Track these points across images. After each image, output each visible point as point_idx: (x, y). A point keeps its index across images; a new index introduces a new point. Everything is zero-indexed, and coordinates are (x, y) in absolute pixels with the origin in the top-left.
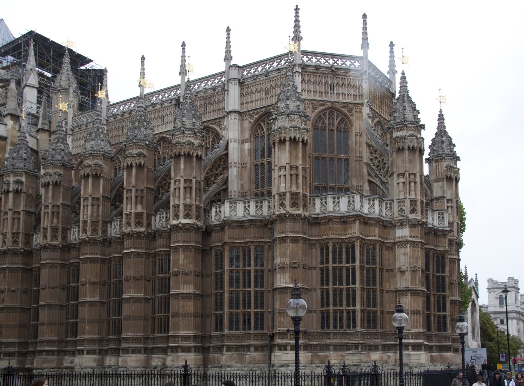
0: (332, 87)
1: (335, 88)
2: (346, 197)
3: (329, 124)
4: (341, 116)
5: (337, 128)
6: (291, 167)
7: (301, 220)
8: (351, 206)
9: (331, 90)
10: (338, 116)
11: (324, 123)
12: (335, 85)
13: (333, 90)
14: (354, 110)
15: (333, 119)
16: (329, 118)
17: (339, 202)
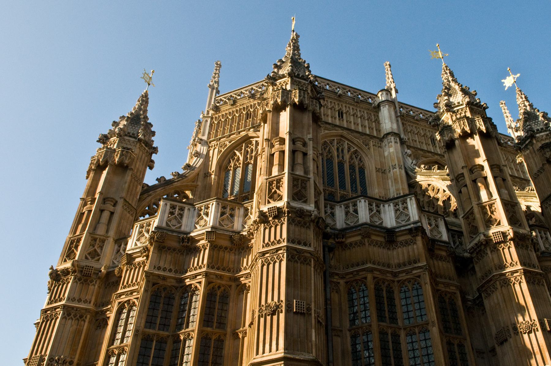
0: (341, 114)
1: (344, 116)
2: (391, 204)
3: (338, 156)
4: (354, 148)
5: (350, 162)
6: (293, 141)
7: (312, 224)
8: (403, 217)
9: (339, 116)
10: (349, 149)
11: (329, 152)
12: (344, 111)
13: (342, 117)
14: (371, 144)
15: (342, 151)
16: (338, 149)
17: (379, 212)
